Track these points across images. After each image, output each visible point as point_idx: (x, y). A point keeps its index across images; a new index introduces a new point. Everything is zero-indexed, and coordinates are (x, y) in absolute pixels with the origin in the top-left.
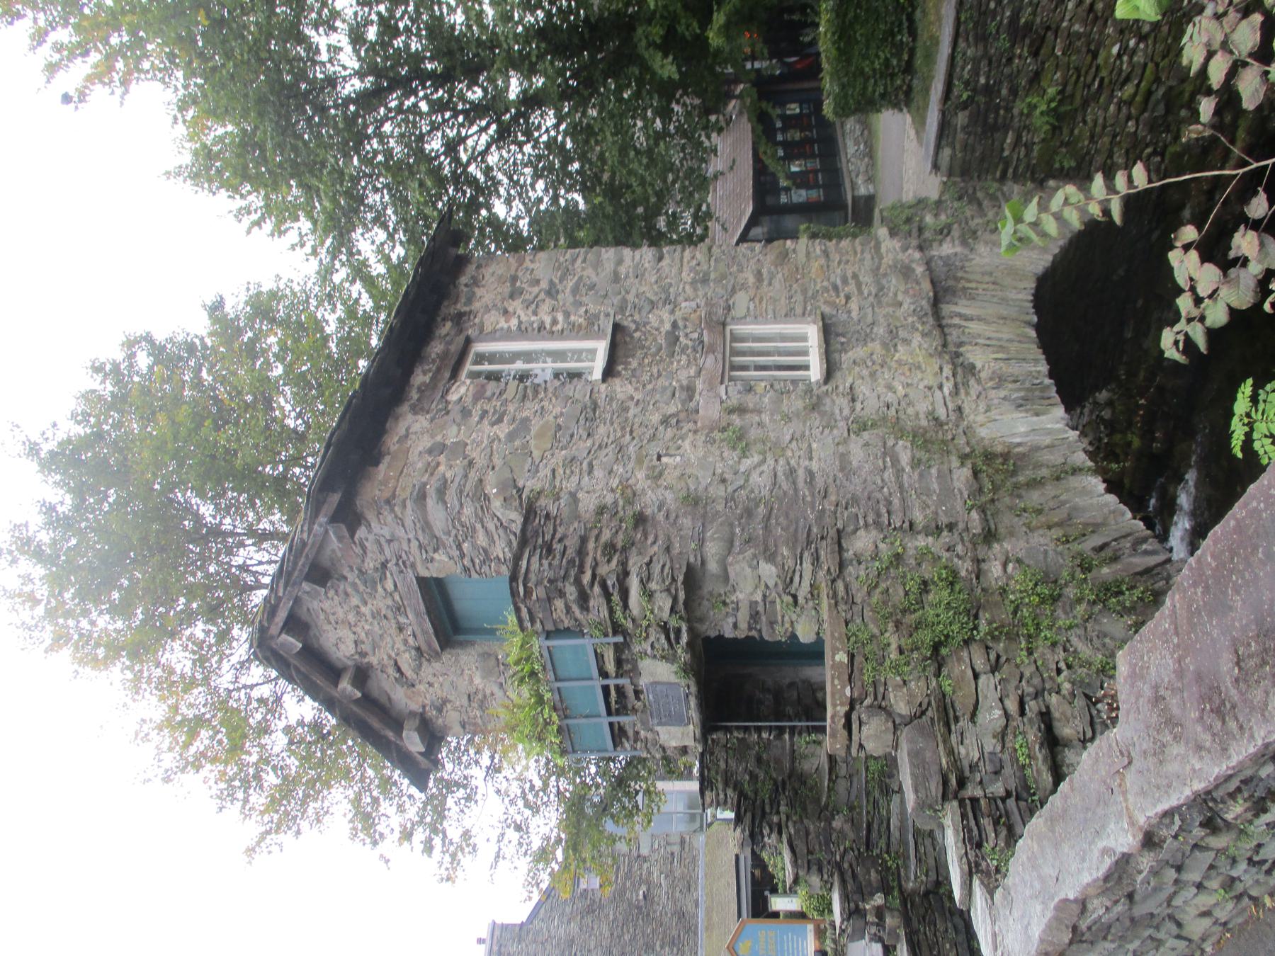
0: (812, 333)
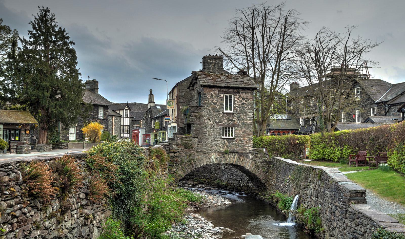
0: (233, 137)
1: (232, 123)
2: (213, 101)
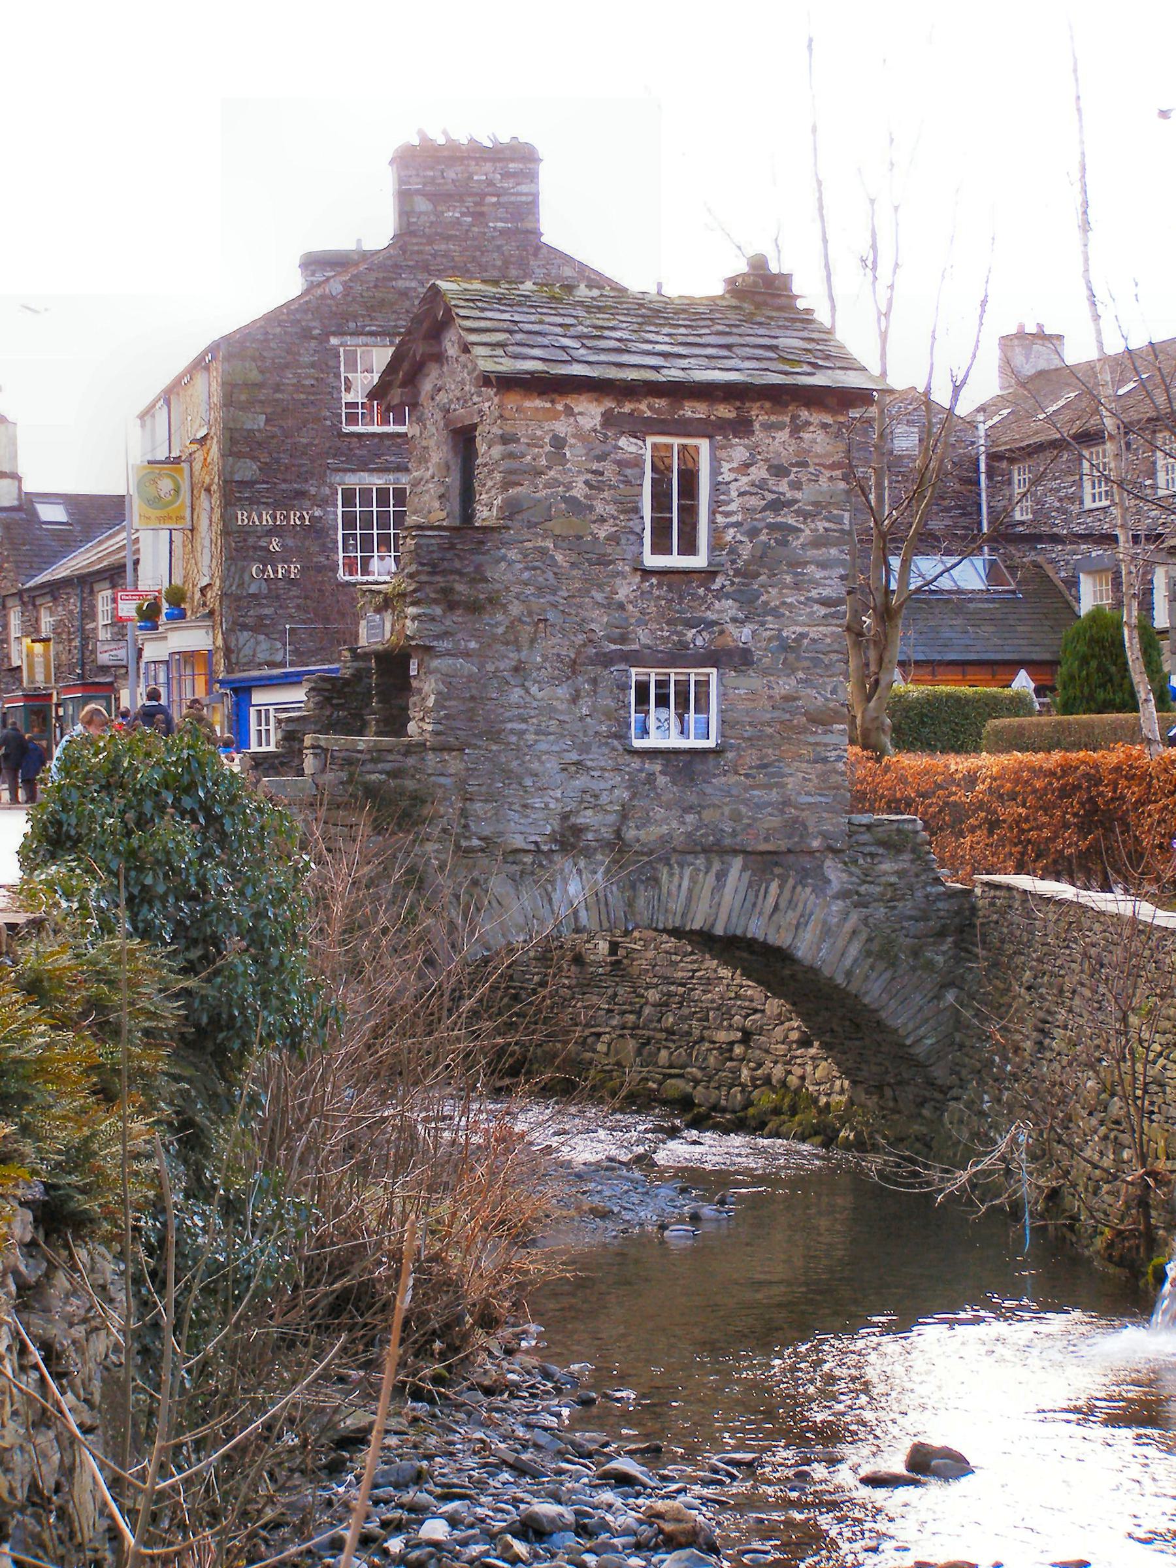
0: (711, 743)
1: (699, 642)
2: (569, 487)
